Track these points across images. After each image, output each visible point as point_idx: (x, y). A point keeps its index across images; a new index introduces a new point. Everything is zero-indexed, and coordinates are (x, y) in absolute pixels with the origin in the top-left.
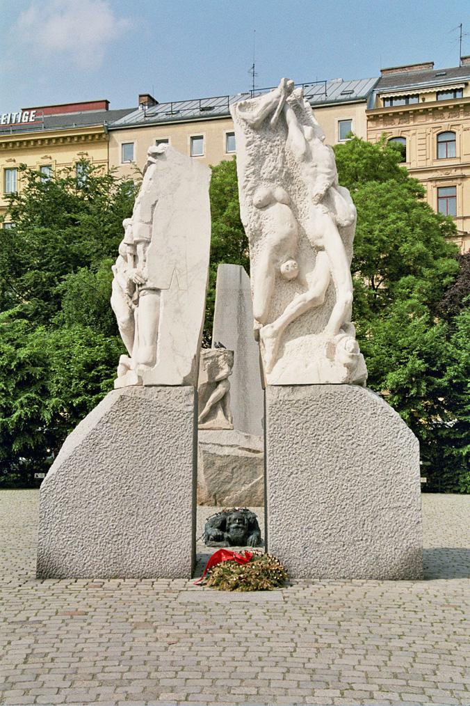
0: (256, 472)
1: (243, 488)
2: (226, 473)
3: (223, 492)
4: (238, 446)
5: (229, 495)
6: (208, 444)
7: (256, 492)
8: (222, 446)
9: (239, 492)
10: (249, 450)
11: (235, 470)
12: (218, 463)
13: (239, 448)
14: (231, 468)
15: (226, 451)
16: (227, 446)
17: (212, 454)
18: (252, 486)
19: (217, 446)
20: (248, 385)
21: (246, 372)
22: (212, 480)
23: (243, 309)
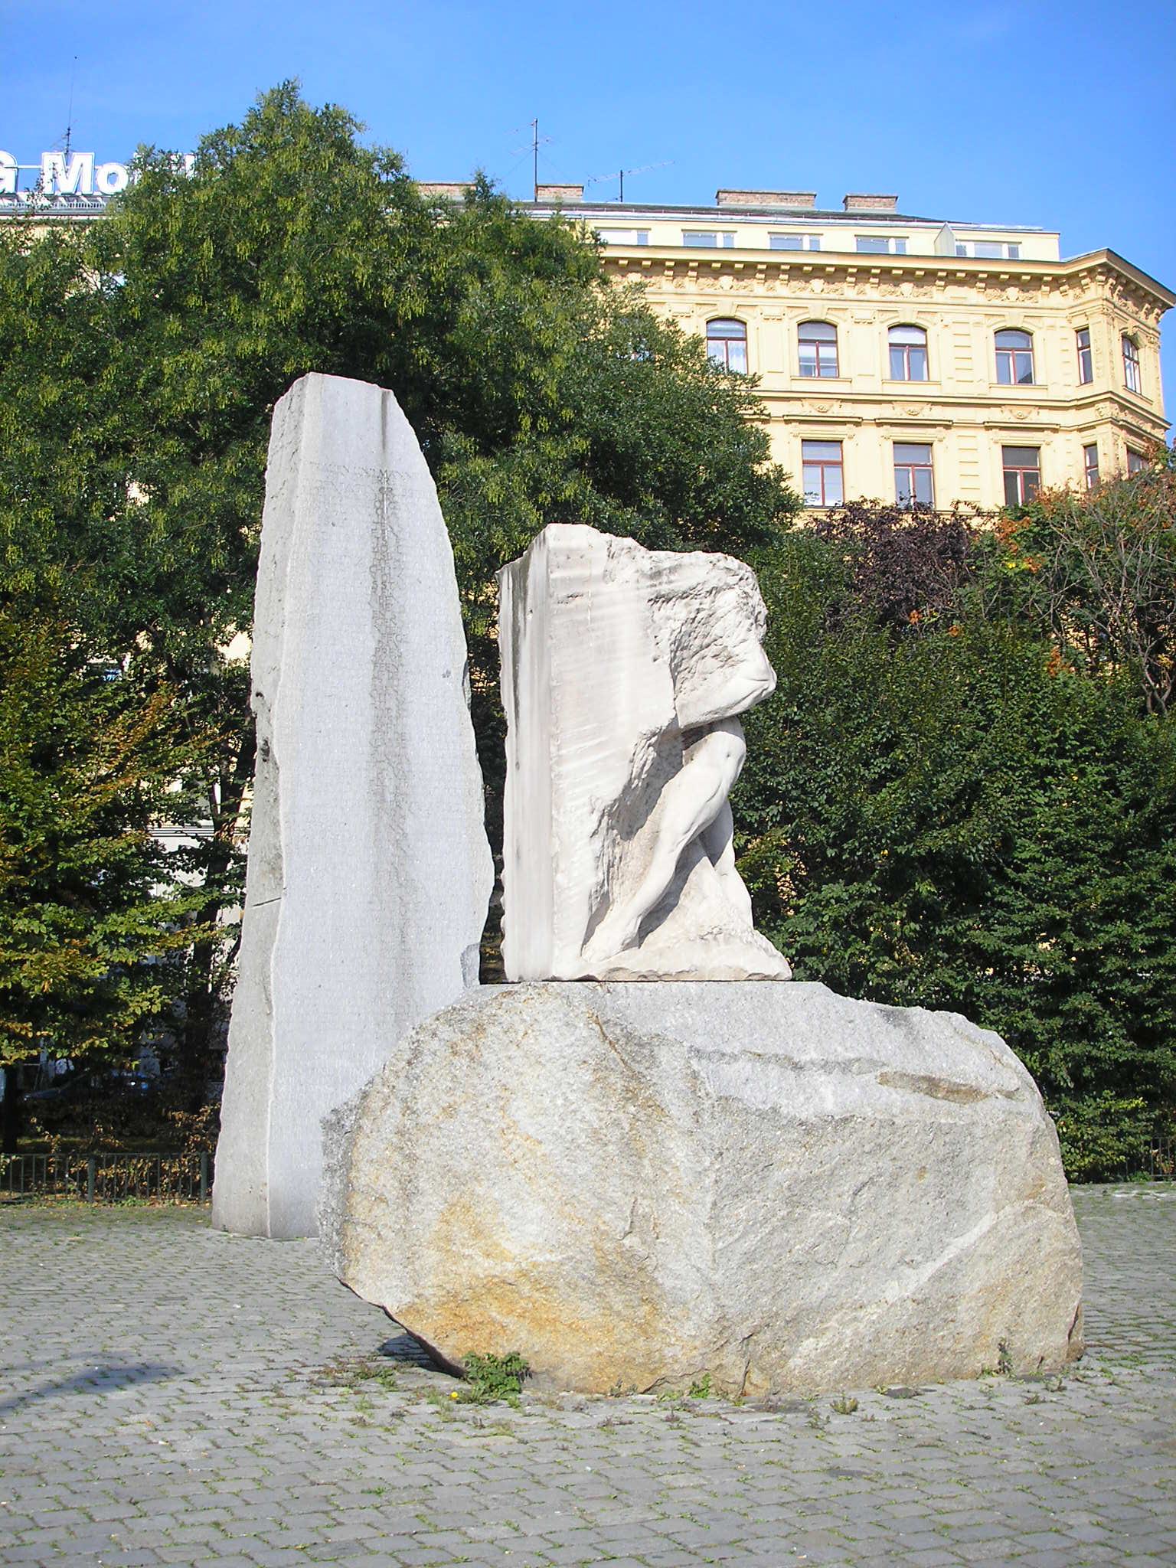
0: (961, 1204)
1: (893, 1291)
2: (823, 1217)
3: (794, 1320)
4: (873, 1063)
5: (819, 1334)
6: (734, 1057)
7: (951, 1302)
8: (797, 1067)
9: (873, 1312)
10: (931, 1085)
11: (866, 1195)
12: (791, 1164)
13: (884, 1080)
14: (848, 1187)
15: (828, 1096)
16: (826, 1066)
17: (762, 1115)
18: (938, 1278)
19: (774, 1071)
20: (410, 825)
21: (402, 776)
22: (750, 1257)
23: (392, 542)
